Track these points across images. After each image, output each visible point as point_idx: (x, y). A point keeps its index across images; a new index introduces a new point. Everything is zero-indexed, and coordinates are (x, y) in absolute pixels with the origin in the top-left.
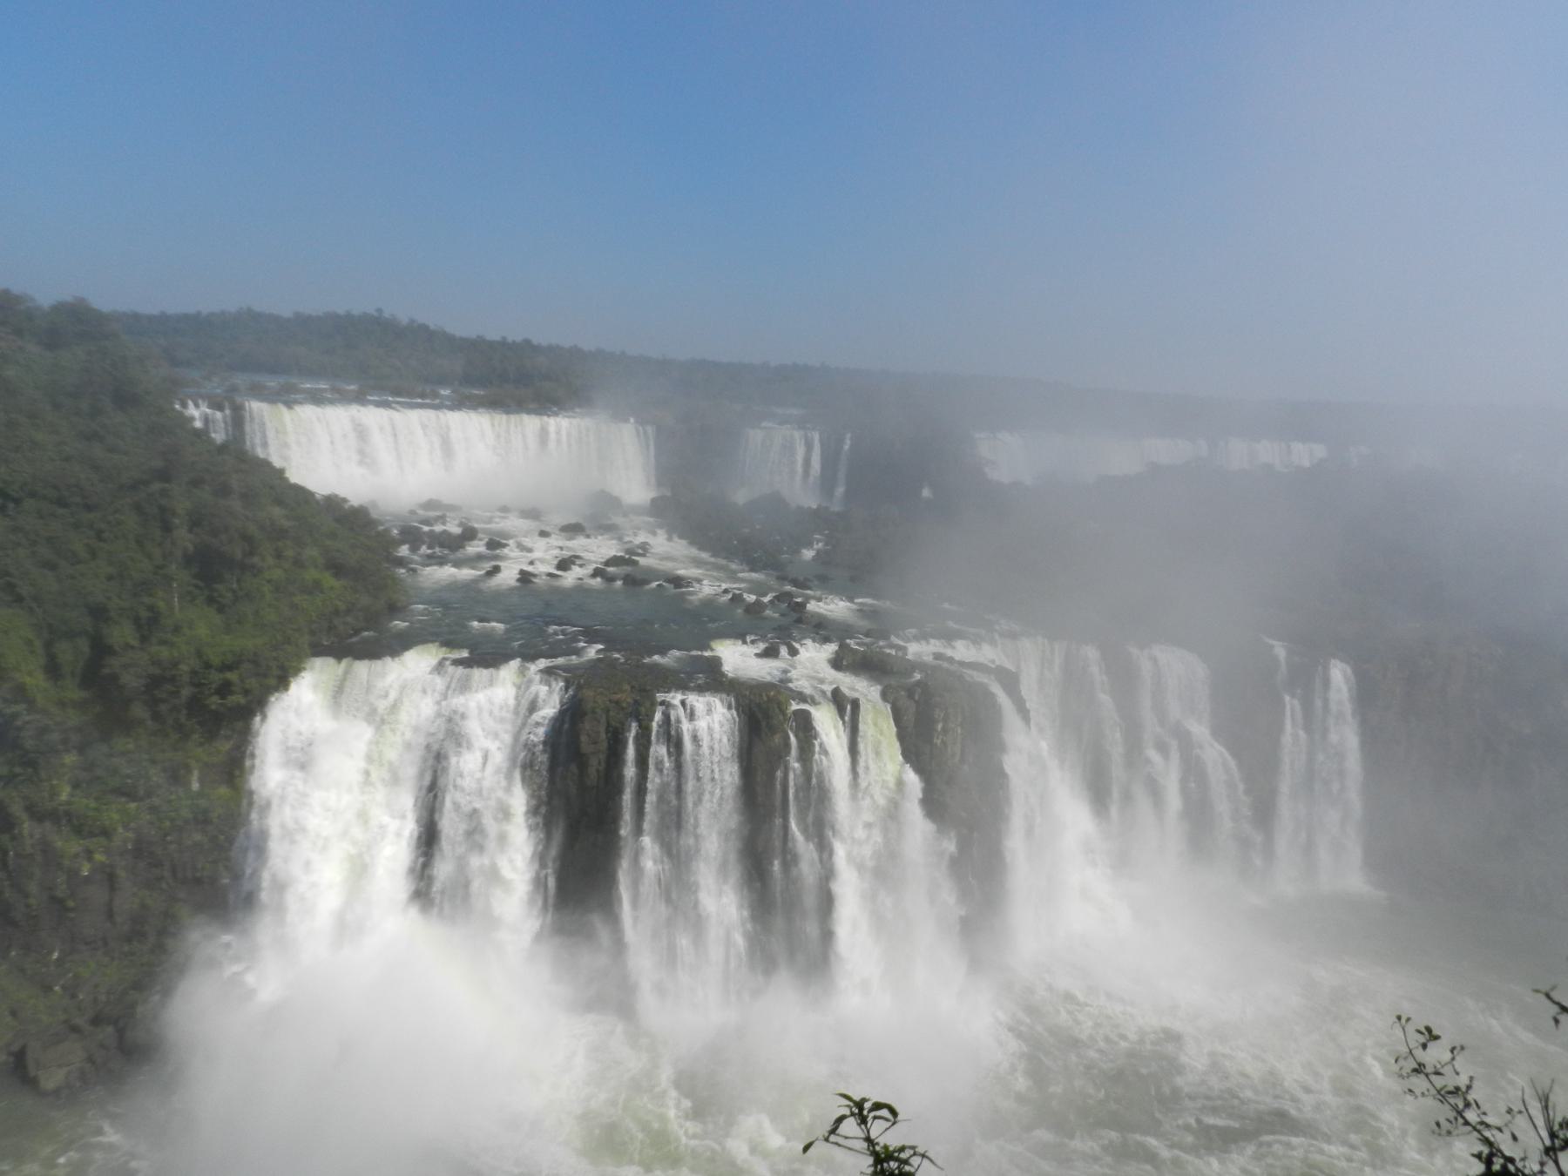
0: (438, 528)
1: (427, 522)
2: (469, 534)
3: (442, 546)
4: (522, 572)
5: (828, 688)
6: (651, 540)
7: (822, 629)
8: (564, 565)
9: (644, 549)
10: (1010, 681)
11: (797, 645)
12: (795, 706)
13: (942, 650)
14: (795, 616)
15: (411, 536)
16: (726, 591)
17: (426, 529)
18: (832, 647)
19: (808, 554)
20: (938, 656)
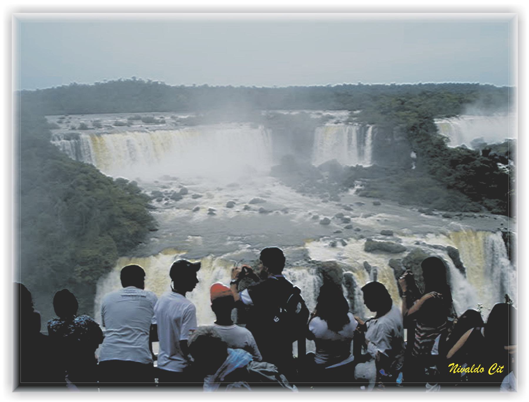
0: (169, 190)
1: (164, 187)
2: (184, 192)
3: (172, 198)
4: (210, 210)
5: (361, 262)
6: (273, 189)
7: (359, 233)
8: (230, 205)
9: (269, 193)
10: (454, 254)
11: (346, 241)
12: (345, 272)
13: (419, 239)
14: (347, 225)
15: (158, 196)
16: (310, 214)
17: (164, 190)
18: (363, 241)
19: (352, 191)
20: (418, 243)
